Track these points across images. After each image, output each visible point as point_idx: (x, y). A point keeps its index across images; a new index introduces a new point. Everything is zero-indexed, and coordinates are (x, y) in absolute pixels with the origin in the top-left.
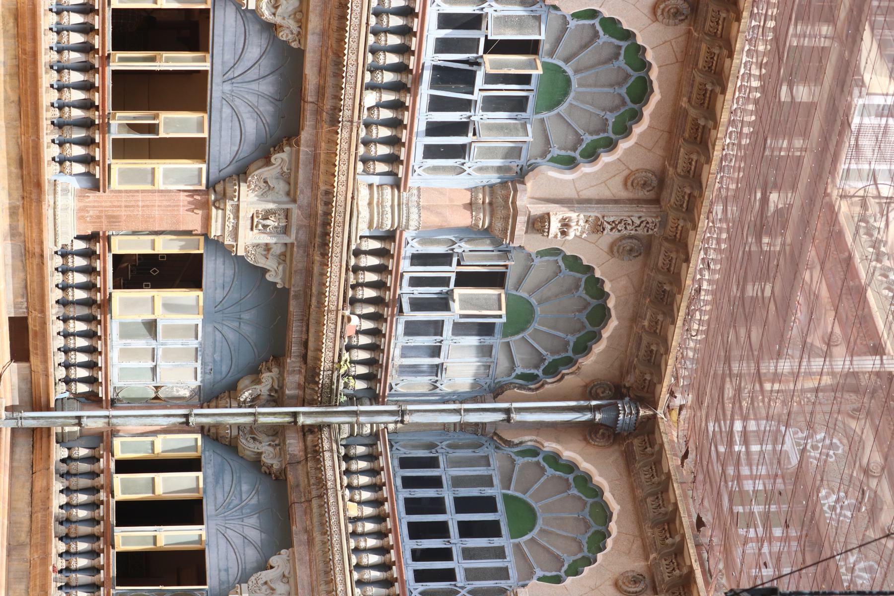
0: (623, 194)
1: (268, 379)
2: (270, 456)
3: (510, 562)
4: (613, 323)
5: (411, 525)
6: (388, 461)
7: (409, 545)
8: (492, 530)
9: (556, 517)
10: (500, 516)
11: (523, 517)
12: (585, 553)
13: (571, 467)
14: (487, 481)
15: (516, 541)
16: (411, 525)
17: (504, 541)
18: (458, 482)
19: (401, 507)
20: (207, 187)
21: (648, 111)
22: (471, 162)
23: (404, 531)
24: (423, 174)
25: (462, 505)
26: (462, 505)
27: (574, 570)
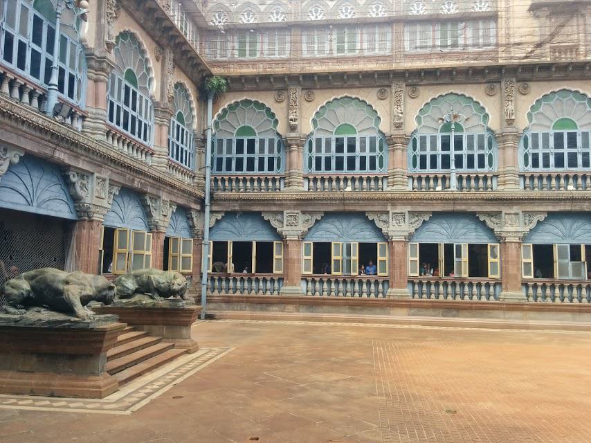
0: (160, 61)
1: (194, 214)
2: (219, 217)
3: (267, 137)
4: (186, 82)
5: (248, 170)
6: (219, 175)
7: (256, 172)
8: (251, 143)
9: (247, 119)
10: (246, 139)
11: (246, 130)
12: (264, 111)
13: (225, 111)
14: (230, 142)
15: (257, 134)
16: (248, 170)
17: (257, 138)
18: (229, 151)
19: (239, 173)
20: (151, 232)
21: (141, 39)
22: (150, 123)
23: (251, 173)
24: (151, 143)
25: (240, 150)
26: (240, 150)
27: (273, 115)
